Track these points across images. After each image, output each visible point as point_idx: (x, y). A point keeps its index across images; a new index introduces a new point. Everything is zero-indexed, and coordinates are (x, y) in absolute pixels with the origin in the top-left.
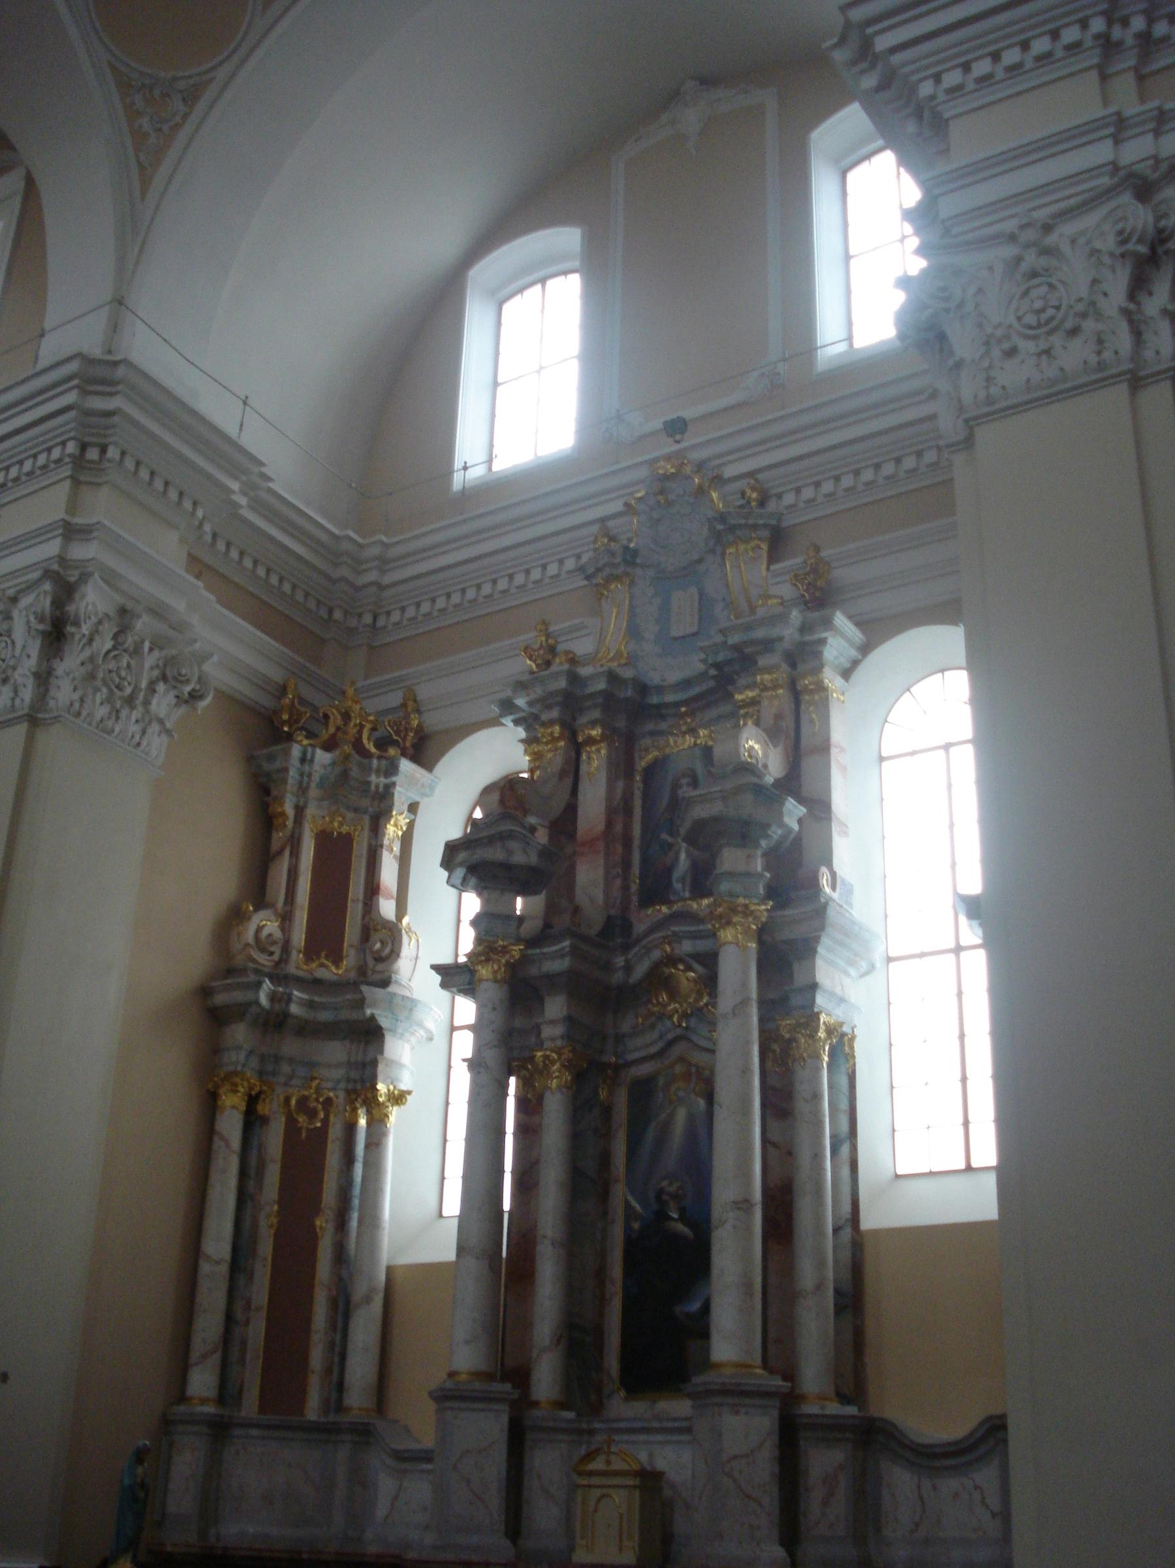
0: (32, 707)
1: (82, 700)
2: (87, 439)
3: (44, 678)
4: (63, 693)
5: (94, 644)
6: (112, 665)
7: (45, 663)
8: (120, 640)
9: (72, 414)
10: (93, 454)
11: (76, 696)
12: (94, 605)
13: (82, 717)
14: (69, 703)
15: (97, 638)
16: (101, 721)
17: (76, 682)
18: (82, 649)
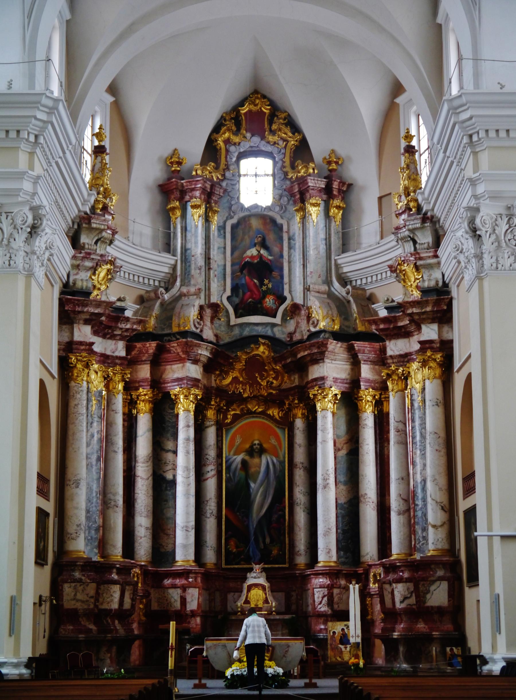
0: (478, 273)
1: (497, 260)
2: (470, 132)
3: (479, 257)
4: (487, 260)
5: (496, 231)
6: (509, 236)
7: (479, 249)
8: (511, 223)
9: (457, 127)
10: (475, 138)
11: (494, 258)
12: (487, 215)
13: (499, 269)
14: (490, 265)
15: (496, 227)
16: (511, 265)
17: (491, 254)
18: (490, 237)
